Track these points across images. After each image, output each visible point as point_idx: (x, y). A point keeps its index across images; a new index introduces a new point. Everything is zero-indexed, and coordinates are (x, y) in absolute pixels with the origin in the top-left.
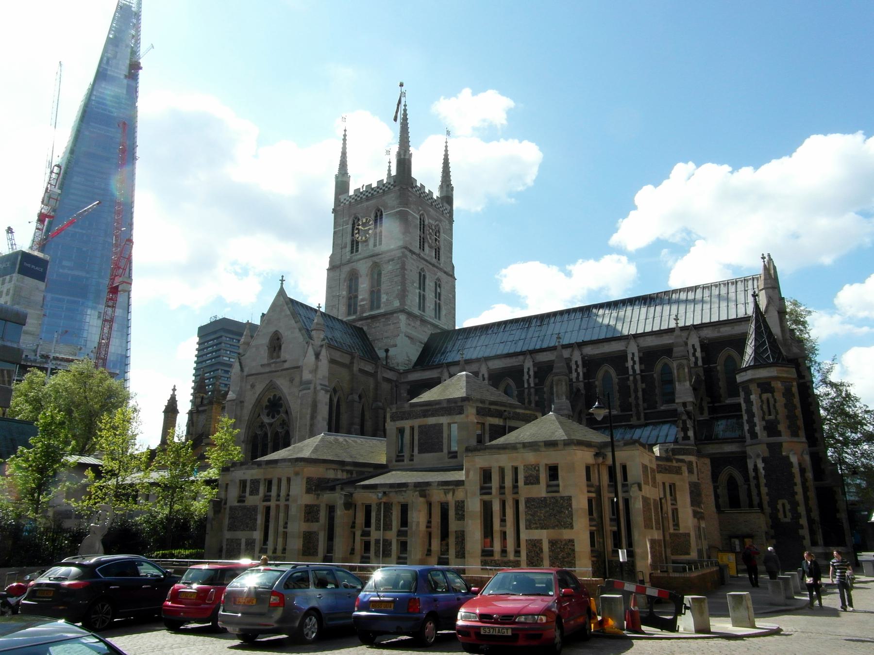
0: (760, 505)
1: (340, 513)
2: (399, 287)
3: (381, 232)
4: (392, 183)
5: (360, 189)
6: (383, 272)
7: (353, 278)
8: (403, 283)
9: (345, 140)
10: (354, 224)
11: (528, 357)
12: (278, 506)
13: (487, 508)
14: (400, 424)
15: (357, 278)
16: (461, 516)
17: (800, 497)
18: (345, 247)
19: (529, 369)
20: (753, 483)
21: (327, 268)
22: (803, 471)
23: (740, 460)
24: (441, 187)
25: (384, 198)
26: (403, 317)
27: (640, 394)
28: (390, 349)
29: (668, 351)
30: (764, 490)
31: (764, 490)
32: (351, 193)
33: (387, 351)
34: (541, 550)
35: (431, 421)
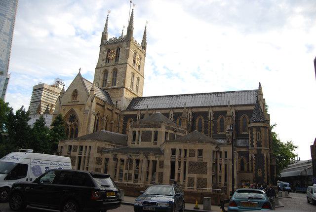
0: (252, 170)
1: (112, 162)
9: (107, 19)
12: (85, 157)
13: (173, 164)
14: (134, 129)
15: (107, 73)
16: (162, 166)
17: (265, 168)
20: (250, 162)
22: (267, 159)
23: (246, 154)
24: (142, 43)
26: (125, 90)
27: (212, 128)
29: (224, 113)
30: (254, 165)
31: (254, 165)
32: (108, 40)
33: (117, 102)
34: (194, 181)
35: (148, 129)
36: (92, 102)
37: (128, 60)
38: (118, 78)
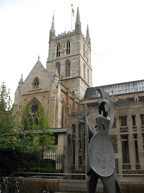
2: (78, 69)
3: (69, 49)
6: (71, 63)
7: (58, 65)
8: (79, 67)
9: (53, 19)
10: (58, 46)
11: (136, 94)
15: (59, 66)
19: (136, 99)
26: (81, 79)
36: (57, 87)
38: (71, 69)
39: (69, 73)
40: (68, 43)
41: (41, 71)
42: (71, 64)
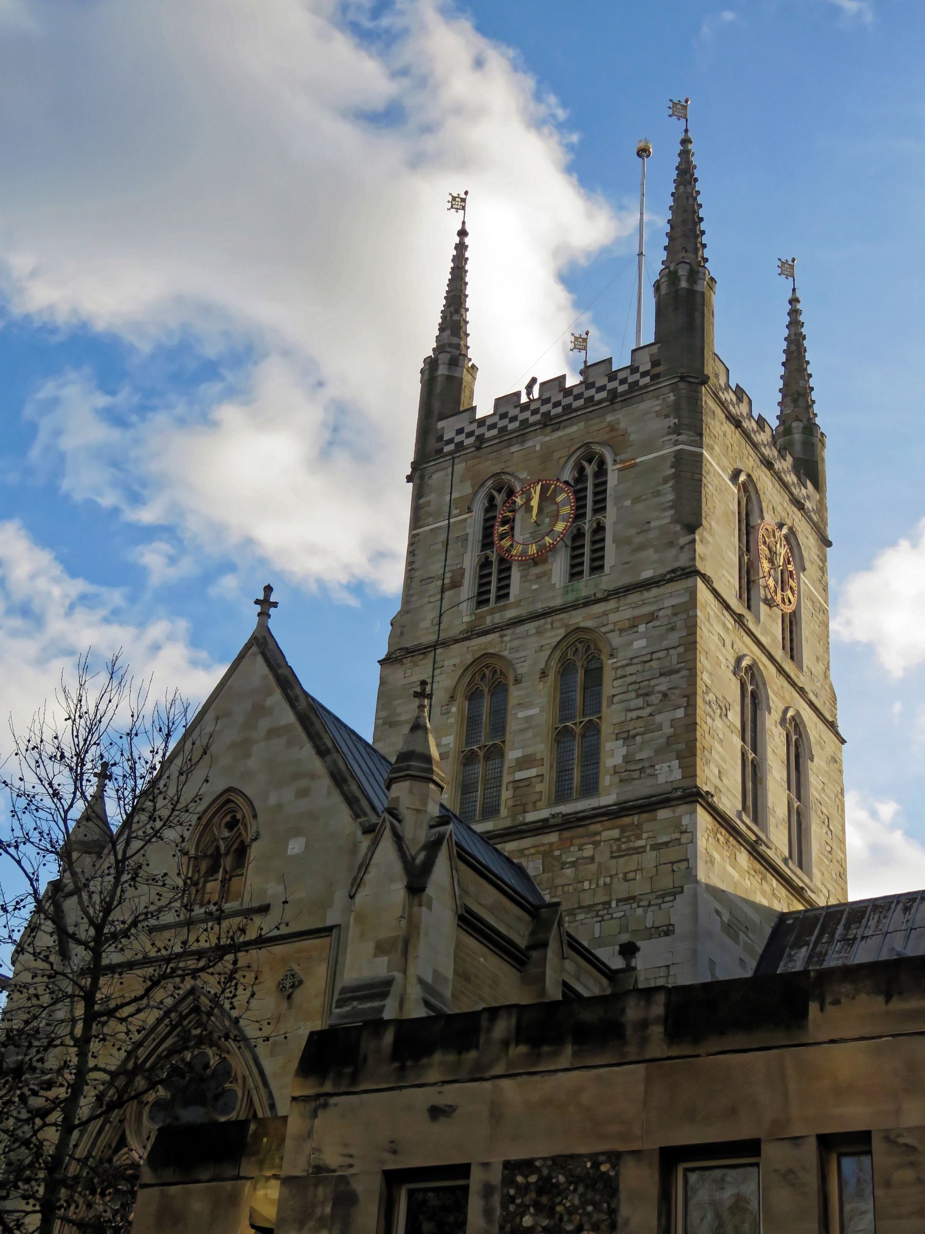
2: (680, 713)
3: (600, 528)
4: (646, 366)
5: (518, 394)
6: (609, 663)
15: (500, 689)
18: (456, 584)
21: (382, 657)
25: (609, 418)
28: (639, 944)
32: (484, 407)
33: (628, 950)
37: (699, 548)
39: (592, 757)
40: (590, 469)
41: (272, 733)
42: (608, 675)
